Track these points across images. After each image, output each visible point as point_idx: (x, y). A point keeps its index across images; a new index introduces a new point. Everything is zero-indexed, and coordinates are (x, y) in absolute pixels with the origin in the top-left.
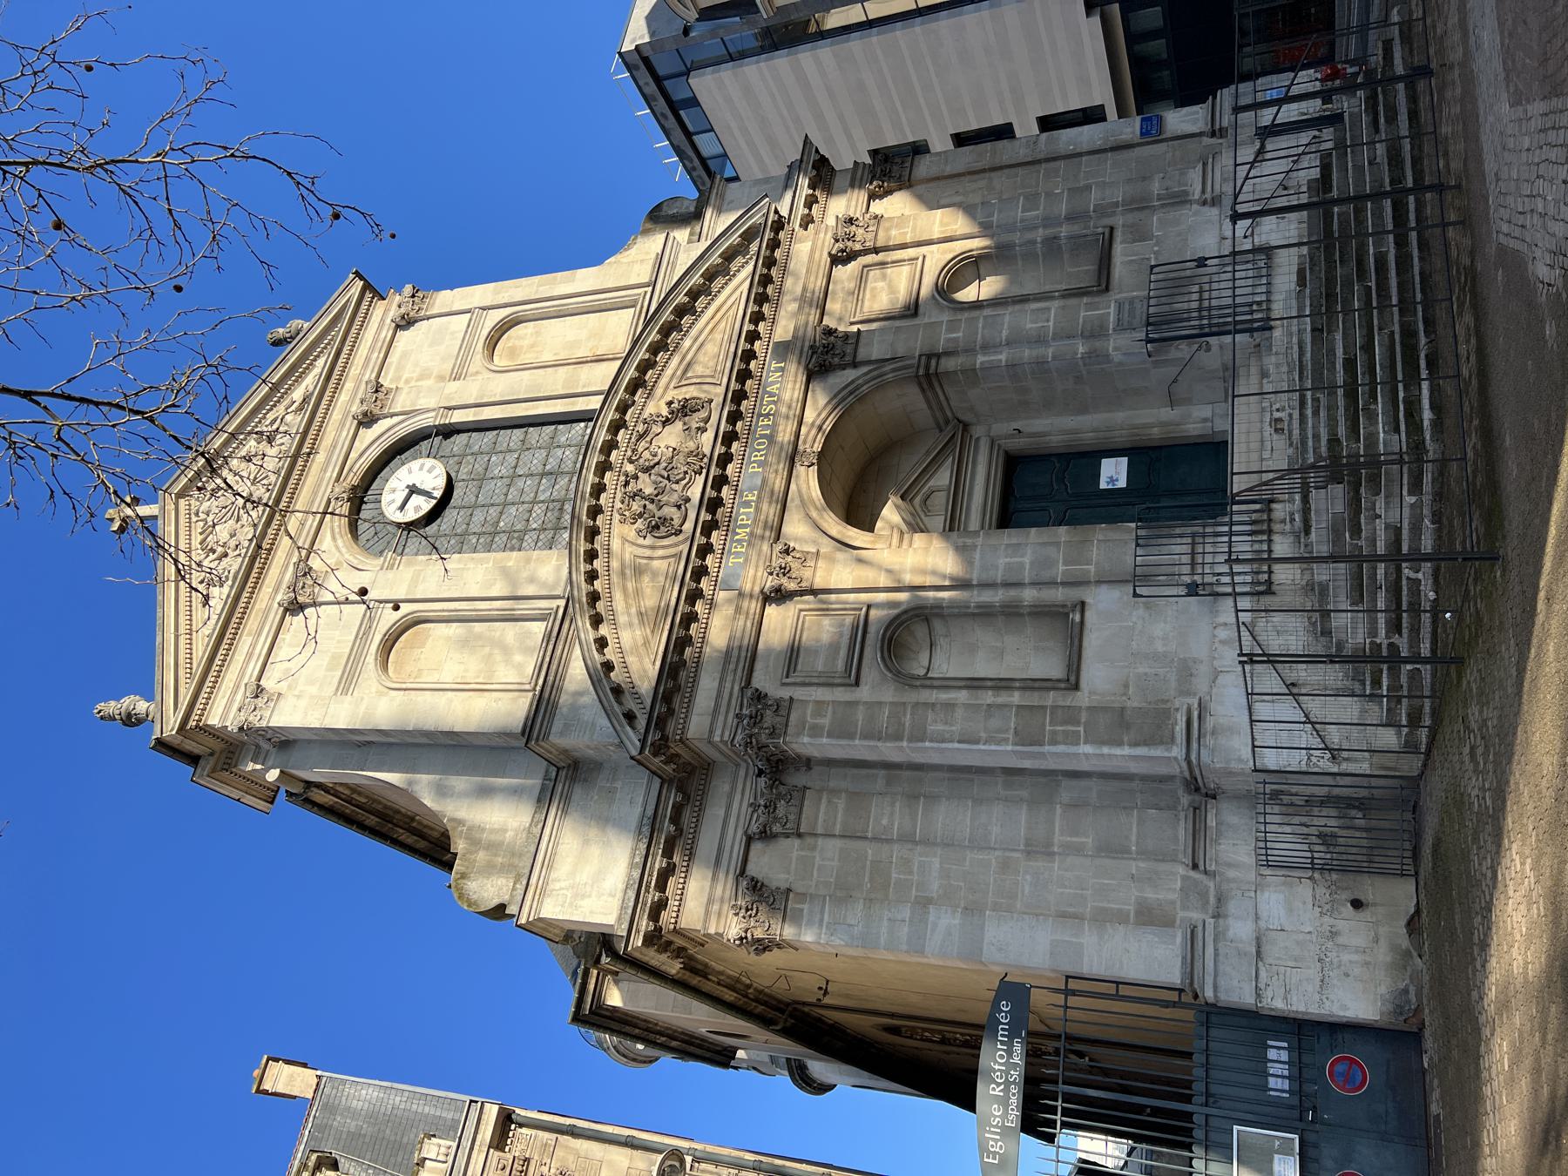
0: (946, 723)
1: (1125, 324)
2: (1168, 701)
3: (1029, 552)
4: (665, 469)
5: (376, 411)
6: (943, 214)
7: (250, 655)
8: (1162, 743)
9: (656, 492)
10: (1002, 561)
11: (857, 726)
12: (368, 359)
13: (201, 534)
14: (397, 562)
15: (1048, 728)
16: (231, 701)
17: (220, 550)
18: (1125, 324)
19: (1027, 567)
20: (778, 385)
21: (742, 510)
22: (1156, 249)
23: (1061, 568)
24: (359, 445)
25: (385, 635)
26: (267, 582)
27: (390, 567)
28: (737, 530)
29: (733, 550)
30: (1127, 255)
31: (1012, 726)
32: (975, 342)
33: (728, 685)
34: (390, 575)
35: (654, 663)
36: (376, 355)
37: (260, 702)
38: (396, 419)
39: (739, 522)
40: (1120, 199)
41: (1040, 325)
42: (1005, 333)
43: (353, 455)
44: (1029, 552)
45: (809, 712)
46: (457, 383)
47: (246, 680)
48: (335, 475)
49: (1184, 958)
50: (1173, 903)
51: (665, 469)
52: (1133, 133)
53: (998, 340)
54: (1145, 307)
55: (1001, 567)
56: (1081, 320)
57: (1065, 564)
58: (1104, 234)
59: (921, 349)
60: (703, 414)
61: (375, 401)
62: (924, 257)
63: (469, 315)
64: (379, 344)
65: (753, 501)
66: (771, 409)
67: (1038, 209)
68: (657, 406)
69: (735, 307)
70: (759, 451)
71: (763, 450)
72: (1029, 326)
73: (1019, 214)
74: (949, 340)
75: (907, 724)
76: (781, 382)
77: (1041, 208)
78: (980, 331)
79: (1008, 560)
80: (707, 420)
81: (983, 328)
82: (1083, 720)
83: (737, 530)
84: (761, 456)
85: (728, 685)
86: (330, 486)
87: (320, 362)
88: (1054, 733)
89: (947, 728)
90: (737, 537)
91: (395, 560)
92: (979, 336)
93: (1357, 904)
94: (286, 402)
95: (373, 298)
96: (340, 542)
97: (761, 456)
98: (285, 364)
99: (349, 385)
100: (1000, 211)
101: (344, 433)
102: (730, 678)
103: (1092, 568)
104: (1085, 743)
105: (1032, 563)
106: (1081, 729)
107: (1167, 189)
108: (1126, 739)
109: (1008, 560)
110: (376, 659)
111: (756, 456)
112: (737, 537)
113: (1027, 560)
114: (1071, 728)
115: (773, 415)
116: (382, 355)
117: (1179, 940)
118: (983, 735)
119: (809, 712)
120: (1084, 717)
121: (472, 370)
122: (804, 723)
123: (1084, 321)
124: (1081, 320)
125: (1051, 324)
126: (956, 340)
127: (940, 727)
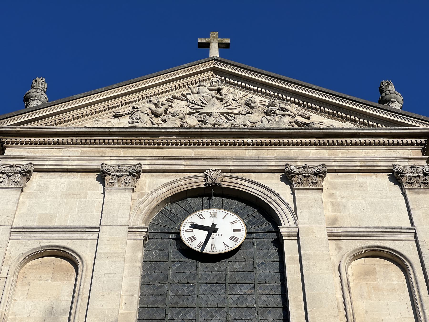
5: (294, 181)
7: (62, 158)
12: (352, 159)
13: (182, 95)
14: (139, 237)
16: (21, 158)
17: (160, 110)
24: (262, 179)
25: (64, 248)
26: (130, 150)
36: (358, 163)
37: (17, 178)
38: (289, 199)
43: (253, 177)
46: (324, 234)
47: (34, 162)
48: (231, 168)
61: (305, 177)
63: (410, 226)
87: (348, 125)
91: (140, 235)
94: (307, 113)
95: (422, 144)
96: (164, 190)
98: (340, 100)
99: (325, 153)
101: (273, 163)
110: (41, 247)
116: (358, 168)
121: (343, 244)
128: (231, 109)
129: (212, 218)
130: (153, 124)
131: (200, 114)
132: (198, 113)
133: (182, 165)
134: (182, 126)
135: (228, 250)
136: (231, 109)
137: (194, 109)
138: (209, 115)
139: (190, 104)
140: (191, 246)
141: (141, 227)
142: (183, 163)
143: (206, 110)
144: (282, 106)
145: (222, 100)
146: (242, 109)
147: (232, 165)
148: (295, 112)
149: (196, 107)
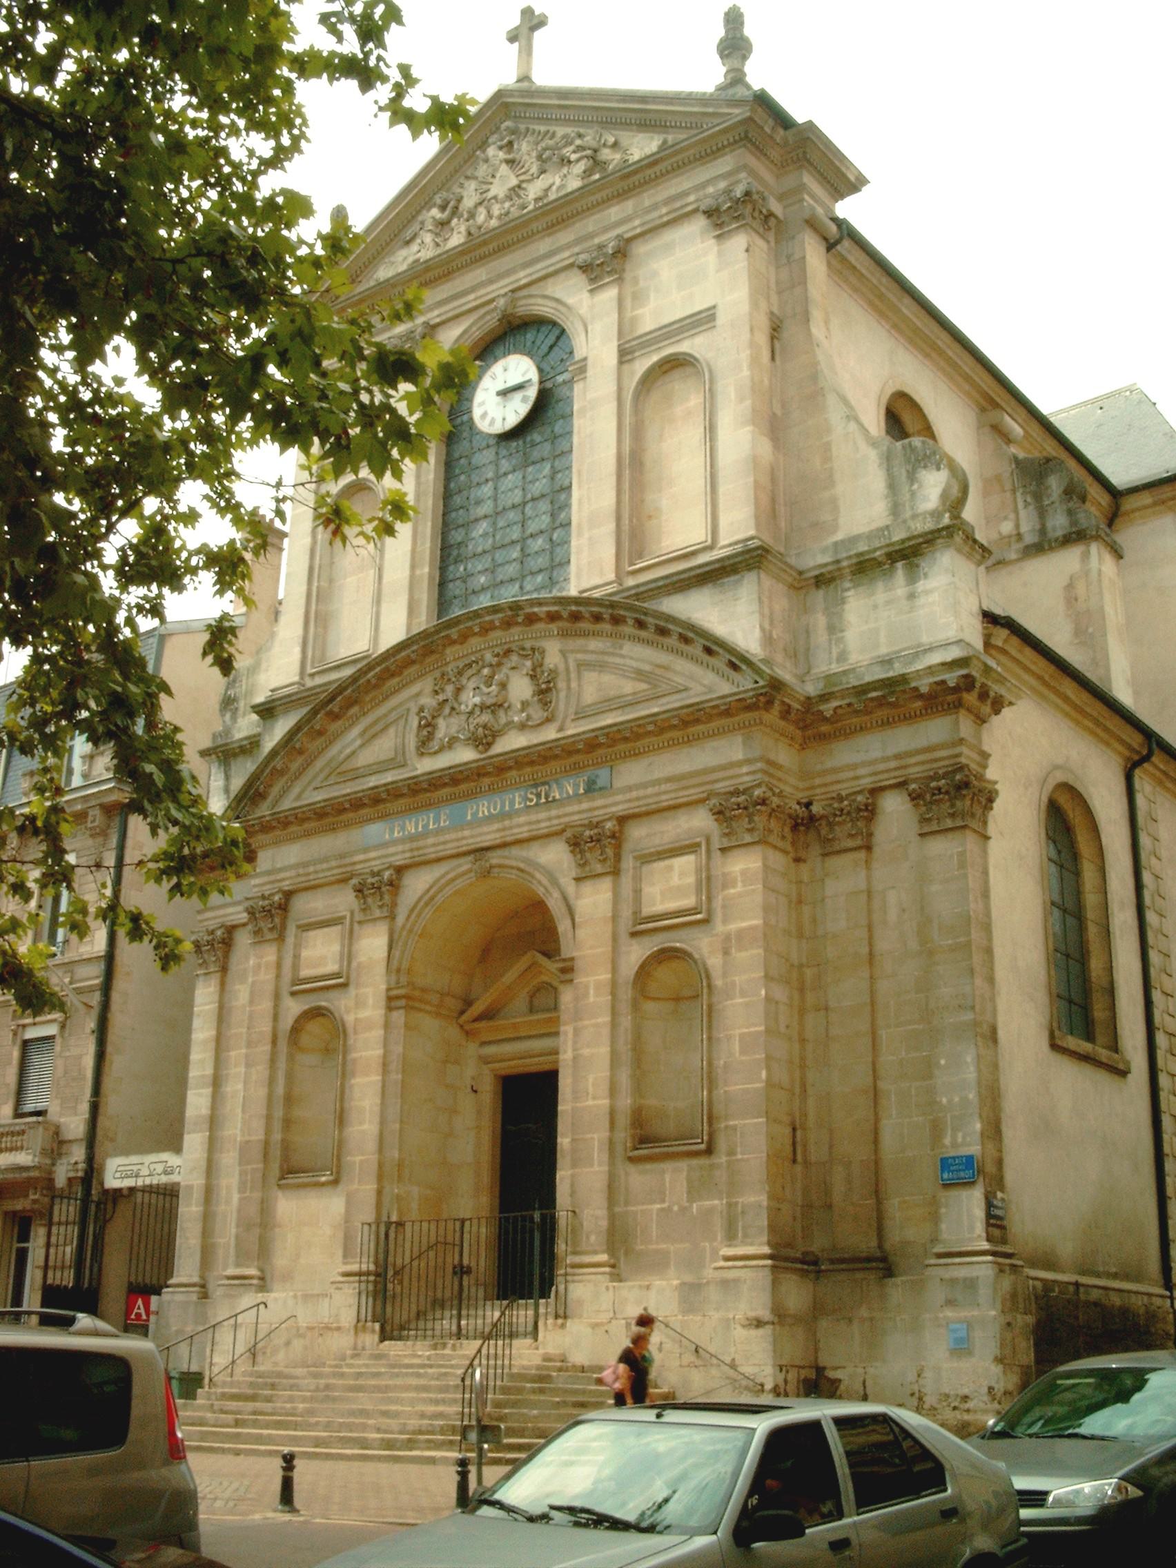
6: (751, 928)
22: (676, 1208)
33: (287, 874)
40: (739, 1157)
41: (591, 1089)
52: (954, 1145)
57: (361, 1161)
60: (537, 714)
62: (706, 921)
64: (678, 204)
66: (531, 800)
67: (742, 1052)
72: (591, 1079)
73: (737, 1032)
74: (587, 987)
77: (743, 1058)
78: (593, 1021)
85: (287, 874)
86: (502, 292)
102: (292, 873)
106: (247, 1194)
107: (743, 1212)
113: (366, 1127)
116: (665, 219)
125: (590, 1102)
126: (586, 995)
127: (254, 1077)
133: (470, 300)
142: (472, 296)
147: (523, 277)
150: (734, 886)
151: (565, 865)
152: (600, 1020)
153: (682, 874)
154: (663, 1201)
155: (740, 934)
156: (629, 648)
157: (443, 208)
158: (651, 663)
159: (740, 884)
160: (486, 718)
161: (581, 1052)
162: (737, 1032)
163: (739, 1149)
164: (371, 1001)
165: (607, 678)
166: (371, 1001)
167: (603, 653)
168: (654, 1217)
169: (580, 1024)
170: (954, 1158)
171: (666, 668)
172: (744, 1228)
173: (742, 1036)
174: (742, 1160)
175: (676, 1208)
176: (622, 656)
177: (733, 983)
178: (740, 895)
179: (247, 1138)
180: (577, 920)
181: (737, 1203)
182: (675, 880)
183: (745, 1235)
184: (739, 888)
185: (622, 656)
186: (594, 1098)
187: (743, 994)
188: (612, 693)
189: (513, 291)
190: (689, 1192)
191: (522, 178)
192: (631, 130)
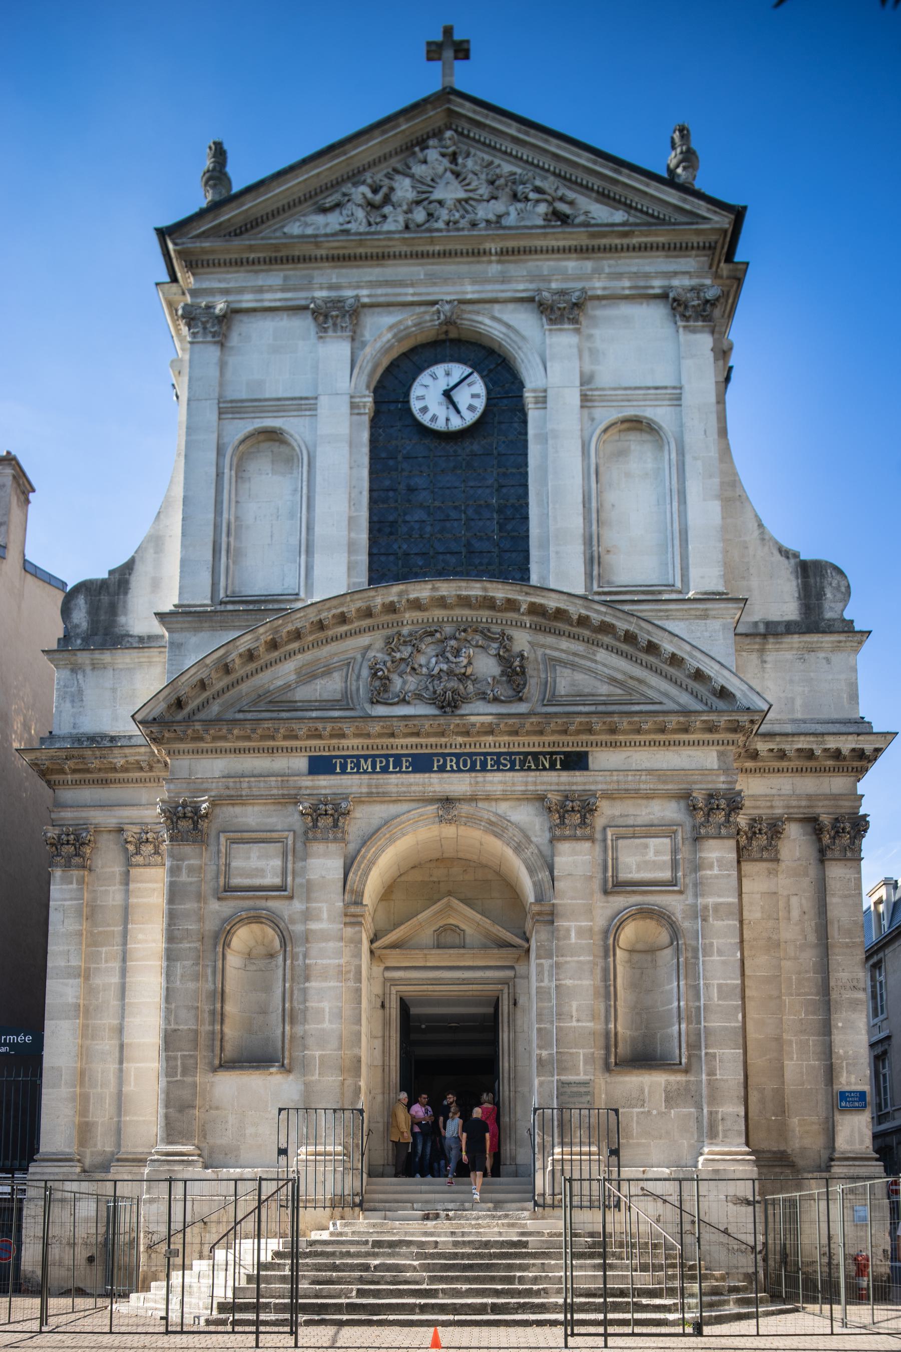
0: (182, 976)
1: (565, 1090)
2: (205, 1138)
3: (334, 1026)
4: (441, 670)
8: (168, 1135)
9: (416, 666)
10: (326, 1005)
11: (180, 904)
15: (179, 1053)
18: (565, 1090)
19: (319, 1026)
20: (533, 767)
21: (391, 760)
22: (655, 1112)
23: (317, 1053)
27: (353, 406)
28: (370, 761)
29: (349, 761)
30: (650, 1086)
31: (181, 1027)
32: (562, 956)
34: (345, 409)
35: (240, 711)
39: (378, 760)
40: (718, 1077)
41: (574, 1014)
42: (568, 982)
44: (334, 1026)
45: (192, 862)
49: (54, 1154)
50: (95, 1145)
51: (441, 670)
53: (561, 977)
54: (580, 1106)
55: (321, 1005)
56: (574, 1050)
57: (321, 1056)
58: (680, 1064)
59: (560, 905)
65: (401, 767)
66: (505, 765)
67: (719, 999)
68: (522, 640)
69: (643, 699)
70: (457, 764)
71: (458, 766)
72: (574, 1005)
73: (716, 982)
74: (568, 930)
75: (181, 945)
76: (537, 770)
77: (720, 1002)
78: (576, 959)
79: (327, 1010)
80: (496, 700)
81: (578, 962)
82: (185, 1079)
83: (370, 761)
84: (451, 766)
86: (448, 298)
88: (175, 1058)
89: (179, 977)
90: (362, 761)
92: (569, 959)
93: (91, 1259)
97: (451, 766)
100: (724, 963)
103: (316, 1077)
104: (168, 1082)
105: (323, 1030)
106: (179, 1078)
107: (722, 1119)
108: (171, 1110)
109: (327, 1010)
111: (451, 761)
112: (362, 761)
113: (326, 1025)
114: (179, 1071)
115: (498, 767)
117: (67, 1150)
118: (173, 1006)
119: (192, 862)
120: (189, 1079)
122: (182, 860)
123: (571, 1054)
124: (574, 1050)
125: (574, 1024)
126: (568, 937)
128: (471, 191)
129: (446, 378)
130: (370, 224)
131: (430, 202)
132: (426, 203)
134: (407, 227)
135: (465, 425)
136: (471, 191)
137: (423, 192)
138: (441, 203)
139: (419, 185)
140: (422, 421)
141: (364, 396)
143: (437, 195)
144: (538, 183)
145: (457, 175)
146: (484, 190)
147: (470, 291)
148: (554, 194)
149: (425, 188)
150: (711, 867)
151: (537, 827)
152: (582, 958)
153: (657, 853)
154: (643, 1106)
155: (717, 907)
156: (602, 655)
157: (375, 191)
158: (624, 673)
159: (716, 868)
160: (453, 684)
161: (563, 982)
162: (716, 982)
163: (718, 1072)
164: (325, 915)
165: (579, 677)
166: (325, 915)
167: (575, 654)
168: (635, 1118)
169: (561, 959)
170: (850, 1092)
171: (640, 681)
172: (724, 1131)
173: (720, 986)
174: (722, 1080)
175: (655, 1112)
176: (595, 661)
177: (711, 944)
178: (717, 877)
179: (173, 1027)
180: (556, 873)
181: (717, 1112)
182: (651, 855)
183: (725, 1136)
184: (716, 871)
185: (595, 661)
186: (578, 1021)
187: (720, 953)
188: (587, 690)
189: (462, 302)
190: (667, 1100)
191: (471, 195)
192: (589, 197)
